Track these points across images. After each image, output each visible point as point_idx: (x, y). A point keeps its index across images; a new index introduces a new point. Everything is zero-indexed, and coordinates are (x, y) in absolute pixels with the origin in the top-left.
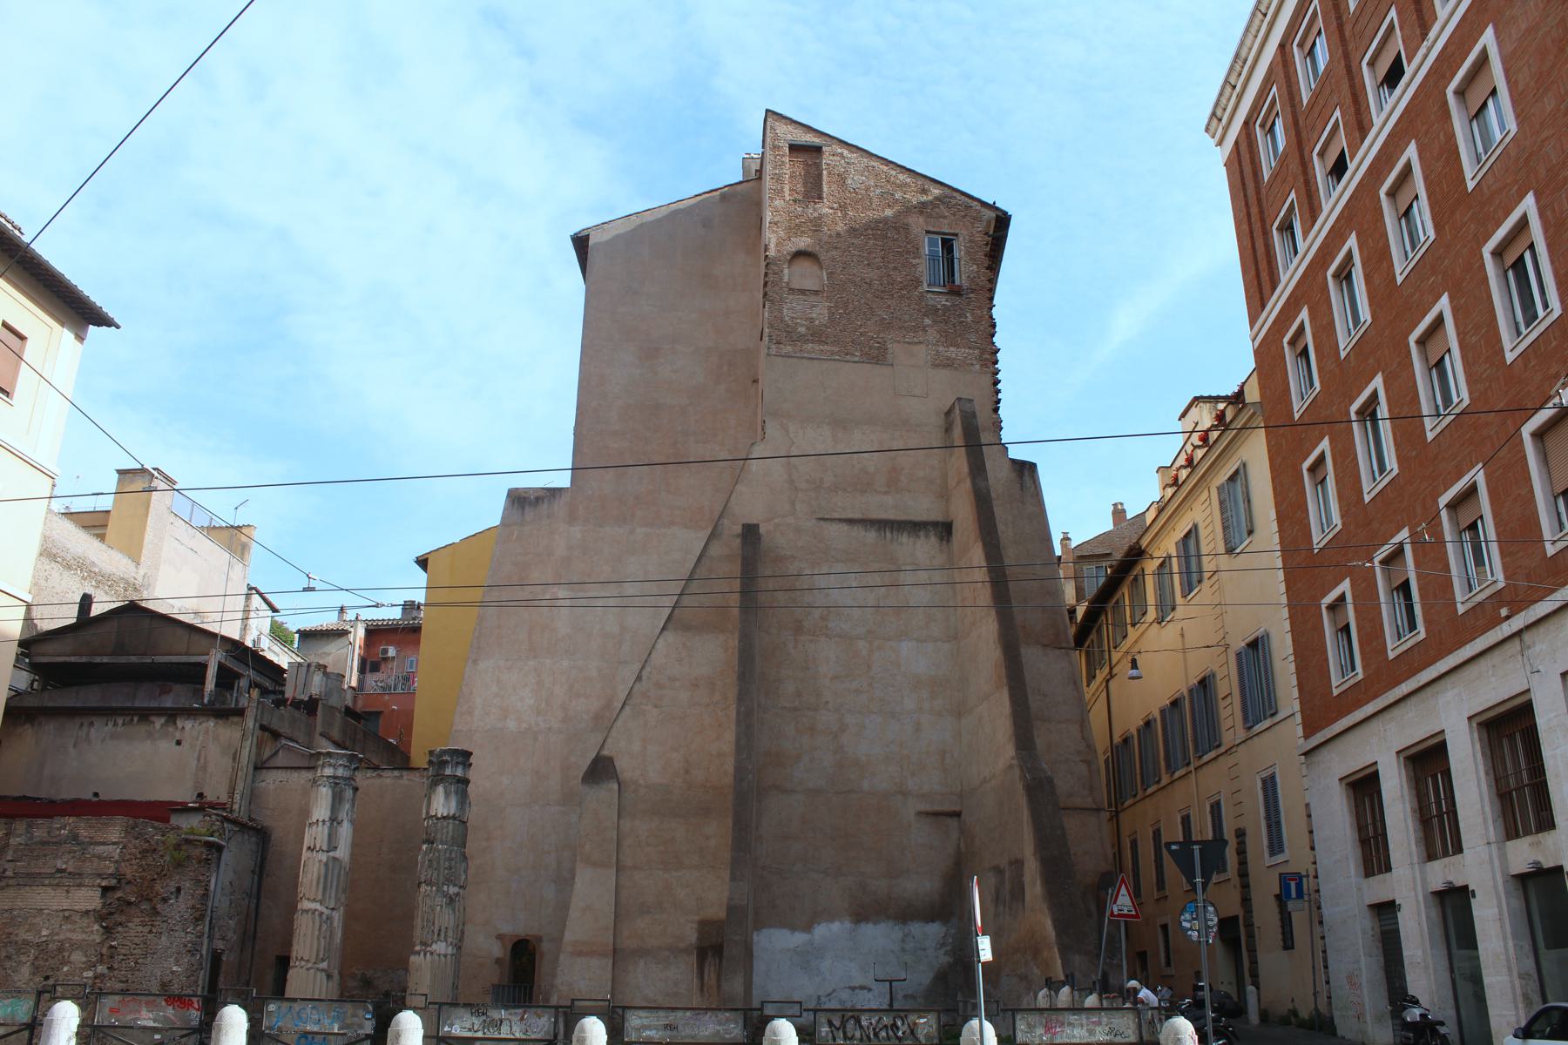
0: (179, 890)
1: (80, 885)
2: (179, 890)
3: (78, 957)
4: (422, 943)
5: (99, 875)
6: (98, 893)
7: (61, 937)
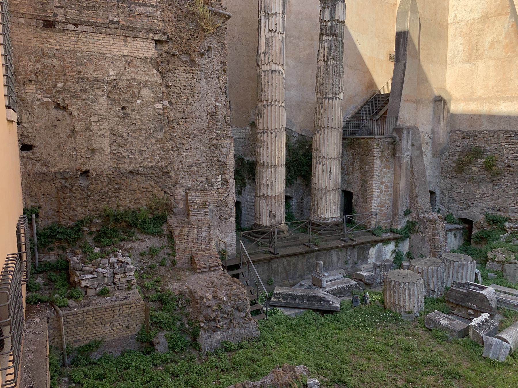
0: (210, 48)
2: (210, 48)
3: (145, 92)
4: (333, 93)
6: (152, 45)
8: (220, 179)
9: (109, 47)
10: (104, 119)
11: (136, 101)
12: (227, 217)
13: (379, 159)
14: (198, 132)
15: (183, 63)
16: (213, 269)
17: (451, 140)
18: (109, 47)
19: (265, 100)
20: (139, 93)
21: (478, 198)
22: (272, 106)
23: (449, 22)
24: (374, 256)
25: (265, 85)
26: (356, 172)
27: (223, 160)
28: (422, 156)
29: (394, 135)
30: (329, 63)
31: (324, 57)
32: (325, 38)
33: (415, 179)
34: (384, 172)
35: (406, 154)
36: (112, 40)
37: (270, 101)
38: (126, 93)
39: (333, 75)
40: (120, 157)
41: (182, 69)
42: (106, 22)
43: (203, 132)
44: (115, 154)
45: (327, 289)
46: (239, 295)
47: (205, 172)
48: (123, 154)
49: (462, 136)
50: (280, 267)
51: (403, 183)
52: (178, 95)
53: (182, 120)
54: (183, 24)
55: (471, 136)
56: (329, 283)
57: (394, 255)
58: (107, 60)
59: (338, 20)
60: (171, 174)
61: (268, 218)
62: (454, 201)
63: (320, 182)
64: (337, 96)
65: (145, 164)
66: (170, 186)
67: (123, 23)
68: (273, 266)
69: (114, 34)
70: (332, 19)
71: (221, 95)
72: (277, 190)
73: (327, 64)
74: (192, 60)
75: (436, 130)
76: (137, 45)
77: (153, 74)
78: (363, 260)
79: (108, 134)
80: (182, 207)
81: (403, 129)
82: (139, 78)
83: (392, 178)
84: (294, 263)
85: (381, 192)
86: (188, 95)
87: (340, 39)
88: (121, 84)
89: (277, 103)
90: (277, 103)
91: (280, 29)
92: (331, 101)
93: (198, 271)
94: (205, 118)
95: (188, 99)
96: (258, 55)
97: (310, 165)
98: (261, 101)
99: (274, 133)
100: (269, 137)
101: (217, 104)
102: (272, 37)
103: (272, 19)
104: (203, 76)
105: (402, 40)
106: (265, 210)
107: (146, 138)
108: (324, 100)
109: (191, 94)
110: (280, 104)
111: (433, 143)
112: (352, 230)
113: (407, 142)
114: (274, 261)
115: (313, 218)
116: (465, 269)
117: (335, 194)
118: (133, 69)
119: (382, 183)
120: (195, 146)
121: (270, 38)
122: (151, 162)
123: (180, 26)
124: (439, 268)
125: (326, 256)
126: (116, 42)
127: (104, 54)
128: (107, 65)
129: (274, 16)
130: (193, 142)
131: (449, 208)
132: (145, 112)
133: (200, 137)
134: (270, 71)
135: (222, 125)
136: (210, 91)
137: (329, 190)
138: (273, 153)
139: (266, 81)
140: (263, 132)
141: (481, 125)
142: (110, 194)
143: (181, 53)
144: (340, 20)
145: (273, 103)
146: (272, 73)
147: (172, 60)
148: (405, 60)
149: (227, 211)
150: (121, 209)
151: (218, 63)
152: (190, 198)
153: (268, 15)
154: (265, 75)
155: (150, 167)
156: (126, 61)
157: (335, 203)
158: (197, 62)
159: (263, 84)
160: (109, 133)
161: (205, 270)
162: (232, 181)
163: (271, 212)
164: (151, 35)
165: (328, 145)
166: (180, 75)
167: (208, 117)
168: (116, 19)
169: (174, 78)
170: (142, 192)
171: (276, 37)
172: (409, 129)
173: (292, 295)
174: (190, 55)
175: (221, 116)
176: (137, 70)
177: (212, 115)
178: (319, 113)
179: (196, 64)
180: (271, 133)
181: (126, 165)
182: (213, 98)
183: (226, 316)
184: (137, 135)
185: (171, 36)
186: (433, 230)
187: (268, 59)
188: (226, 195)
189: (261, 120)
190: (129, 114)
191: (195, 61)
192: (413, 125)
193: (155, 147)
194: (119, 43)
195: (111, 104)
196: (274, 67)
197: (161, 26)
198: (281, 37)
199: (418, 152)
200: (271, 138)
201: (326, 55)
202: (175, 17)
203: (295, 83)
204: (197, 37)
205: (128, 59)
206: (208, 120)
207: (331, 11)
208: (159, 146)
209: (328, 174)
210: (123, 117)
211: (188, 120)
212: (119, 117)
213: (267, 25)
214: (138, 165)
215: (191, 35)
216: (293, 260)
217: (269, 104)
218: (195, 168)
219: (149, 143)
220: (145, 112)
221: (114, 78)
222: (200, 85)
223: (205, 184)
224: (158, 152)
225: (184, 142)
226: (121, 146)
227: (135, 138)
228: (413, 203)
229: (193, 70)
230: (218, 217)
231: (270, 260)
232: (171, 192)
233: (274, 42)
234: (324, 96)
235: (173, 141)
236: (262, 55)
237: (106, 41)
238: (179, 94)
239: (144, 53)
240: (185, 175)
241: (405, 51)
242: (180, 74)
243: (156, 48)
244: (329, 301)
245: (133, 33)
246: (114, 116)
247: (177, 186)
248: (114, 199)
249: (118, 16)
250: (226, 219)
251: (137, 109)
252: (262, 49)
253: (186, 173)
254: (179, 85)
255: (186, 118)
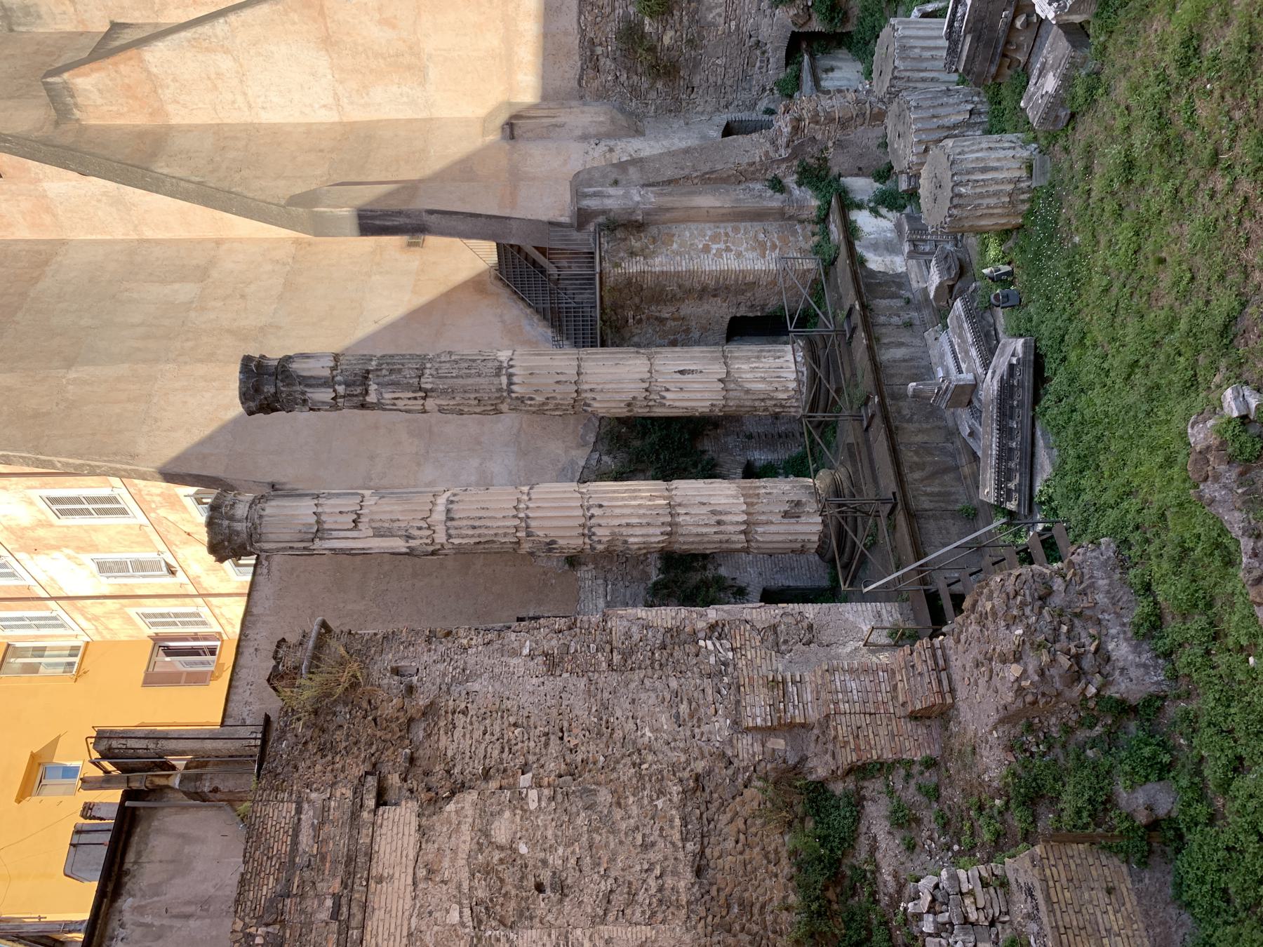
0: (396, 671)
1: (370, 856)
2: (396, 671)
3: (502, 831)
4: (498, 375)
5: (355, 816)
6: (388, 812)
7: (465, 874)
8: (709, 643)
9: (393, 921)
10: (567, 937)
11: (522, 856)
12: (805, 625)
13: (650, 261)
14: (592, 700)
15: (429, 735)
16: (941, 662)
17: (602, 95)
18: (393, 921)
19: (514, 535)
20: (501, 848)
21: (737, 26)
22: (528, 517)
23: (336, 119)
24: (888, 259)
25: (479, 536)
26: (682, 313)
27: (660, 636)
28: (641, 160)
29: (592, 229)
30: (429, 386)
31: (415, 398)
32: (372, 398)
33: (695, 174)
34: (680, 246)
35: (637, 198)
36: (377, 912)
37: (517, 522)
38: (502, 881)
39: (456, 377)
40: (660, 901)
41: (443, 738)
42: (334, 926)
43: (593, 688)
44: (653, 914)
45: (980, 370)
46: (1008, 595)
47: (692, 681)
48: (653, 891)
49: (591, 73)
50: (929, 489)
51: (707, 201)
52: (507, 749)
53: (566, 739)
54: (339, 735)
55: (592, 52)
56: (964, 366)
57: (883, 211)
58: (424, 928)
59: (333, 369)
60: (700, 770)
61: (803, 519)
62: (746, 77)
63: (706, 395)
64: (505, 364)
65: (677, 837)
66: (730, 772)
67: (336, 886)
68: (927, 505)
69: (364, 907)
70: (328, 383)
71: (506, 641)
72: (732, 501)
73: (432, 390)
74: (424, 714)
75: (578, 132)
76: (388, 851)
77: (456, 812)
78: (900, 285)
79: (606, 931)
80: (782, 742)
81: (579, 209)
82: (466, 847)
83: (693, 226)
84: (916, 453)
85: (728, 250)
86: (506, 724)
87: (374, 363)
88: (481, 894)
89: (522, 506)
90: (522, 506)
91: (351, 504)
92: (515, 379)
93: (949, 701)
94: (559, 682)
95: (515, 725)
96: (411, 553)
97: (668, 421)
98: (518, 543)
99: (595, 511)
100: (602, 522)
101: (526, 651)
102: (372, 520)
103: (329, 522)
104: (461, 688)
105: (377, 222)
106: (782, 529)
107: (613, 831)
108: (513, 395)
109: (502, 717)
110: (525, 497)
111: (609, 136)
112: (825, 314)
113: (609, 196)
114: (913, 505)
115: (797, 409)
116: (913, 42)
117: (737, 358)
118: (446, 863)
119: (706, 249)
120: (628, 707)
121: (374, 525)
122: (672, 821)
123: (344, 744)
124: (913, 103)
125: (892, 376)
126: (383, 904)
127: (410, 935)
128: (436, 928)
129: (323, 518)
130: (619, 713)
131: (764, 90)
132: (549, 833)
133: (606, 695)
134: (449, 524)
135: (576, 639)
136: (496, 670)
137: (728, 372)
138: (641, 512)
139: (470, 532)
140: (590, 537)
141: (566, 33)
142: (755, 928)
143: (407, 742)
144: (332, 364)
145: (522, 515)
146: (452, 519)
147: (423, 763)
148: (420, 212)
149: (788, 625)
150: (792, 899)
151: (429, 650)
152: (759, 720)
153: (320, 532)
154: (459, 536)
155: (685, 823)
156: (427, 879)
157: (758, 357)
158: (427, 701)
159: (477, 540)
160: (601, 927)
161: (945, 683)
162: (713, 613)
163: (786, 515)
164: (365, 815)
165: (620, 382)
166: (460, 743)
167: (558, 673)
168: (329, 903)
169: (467, 760)
170: (747, 845)
171: (372, 513)
172: (578, 194)
173: (1000, 458)
174: (411, 720)
175: (554, 642)
176: (448, 852)
177: (553, 664)
178: (544, 404)
179: (432, 703)
180: (592, 516)
181: (682, 884)
182: (514, 661)
183: (1064, 628)
184: (604, 855)
185: (366, 767)
186: (817, 123)
187: (420, 528)
188: (748, 627)
189: (561, 542)
190: (554, 873)
191: (426, 707)
192: (568, 187)
193: (635, 810)
194: (383, 897)
195: (531, 918)
196: (439, 516)
197: (344, 790)
198: (370, 501)
199: (632, 170)
200: (602, 516)
201: (411, 395)
202: (324, 756)
203: (475, 462)
204: (369, 702)
205: (422, 873)
206: (565, 675)
207: (307, 385)
208: (631, 799)
209: (687, 378)
210: (562, 889)
211: (566, 724)
212: (561, 901)
213: (342, 534)
214: (681, 855)
215: (365, 718)
216: (908, 457)
217: (523, 524)
218: (684, 708)
219: (623, 826)
220: (549, 833)
221: (467, 912)
222: (481, 695)
223: (721, 681)
224: (646, 802)
225: (618, 734)
226: (632, 895)
227: (612, 860)
228: (753, 173)
229: (446, 712)
230: (806, 648)
231: (912, 516)
232: (746, 769)
233: (384, 517)
234: (505, 394)
235: (618, 762)
236: (413, 543)
237: (380, 929)
238: (503, 748)
239: (407, 833)
240: (702, 734)
241: (400, 213)
242: (455, 744)
243: (396, 804)
244: (1011, 366)
245: (361, 860)
246: (560, 912)
247: (729, 753)
248: (769, 918)
249: (320, 897)
250: (810, 627)
251: (542, 855)
252: (399, 545)
253: (697, 730)
254: (483, 746)
255: (562, 731)
